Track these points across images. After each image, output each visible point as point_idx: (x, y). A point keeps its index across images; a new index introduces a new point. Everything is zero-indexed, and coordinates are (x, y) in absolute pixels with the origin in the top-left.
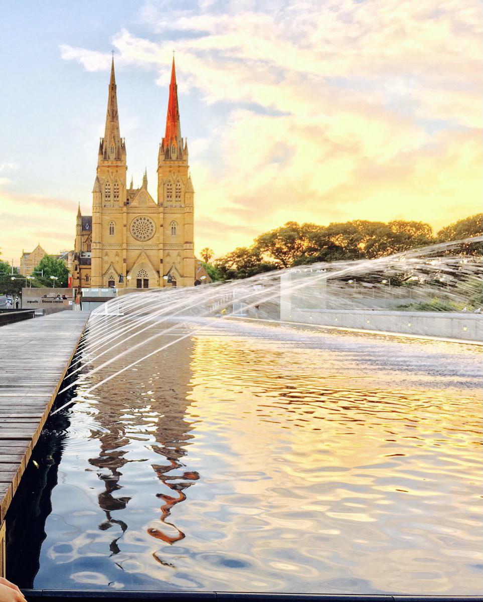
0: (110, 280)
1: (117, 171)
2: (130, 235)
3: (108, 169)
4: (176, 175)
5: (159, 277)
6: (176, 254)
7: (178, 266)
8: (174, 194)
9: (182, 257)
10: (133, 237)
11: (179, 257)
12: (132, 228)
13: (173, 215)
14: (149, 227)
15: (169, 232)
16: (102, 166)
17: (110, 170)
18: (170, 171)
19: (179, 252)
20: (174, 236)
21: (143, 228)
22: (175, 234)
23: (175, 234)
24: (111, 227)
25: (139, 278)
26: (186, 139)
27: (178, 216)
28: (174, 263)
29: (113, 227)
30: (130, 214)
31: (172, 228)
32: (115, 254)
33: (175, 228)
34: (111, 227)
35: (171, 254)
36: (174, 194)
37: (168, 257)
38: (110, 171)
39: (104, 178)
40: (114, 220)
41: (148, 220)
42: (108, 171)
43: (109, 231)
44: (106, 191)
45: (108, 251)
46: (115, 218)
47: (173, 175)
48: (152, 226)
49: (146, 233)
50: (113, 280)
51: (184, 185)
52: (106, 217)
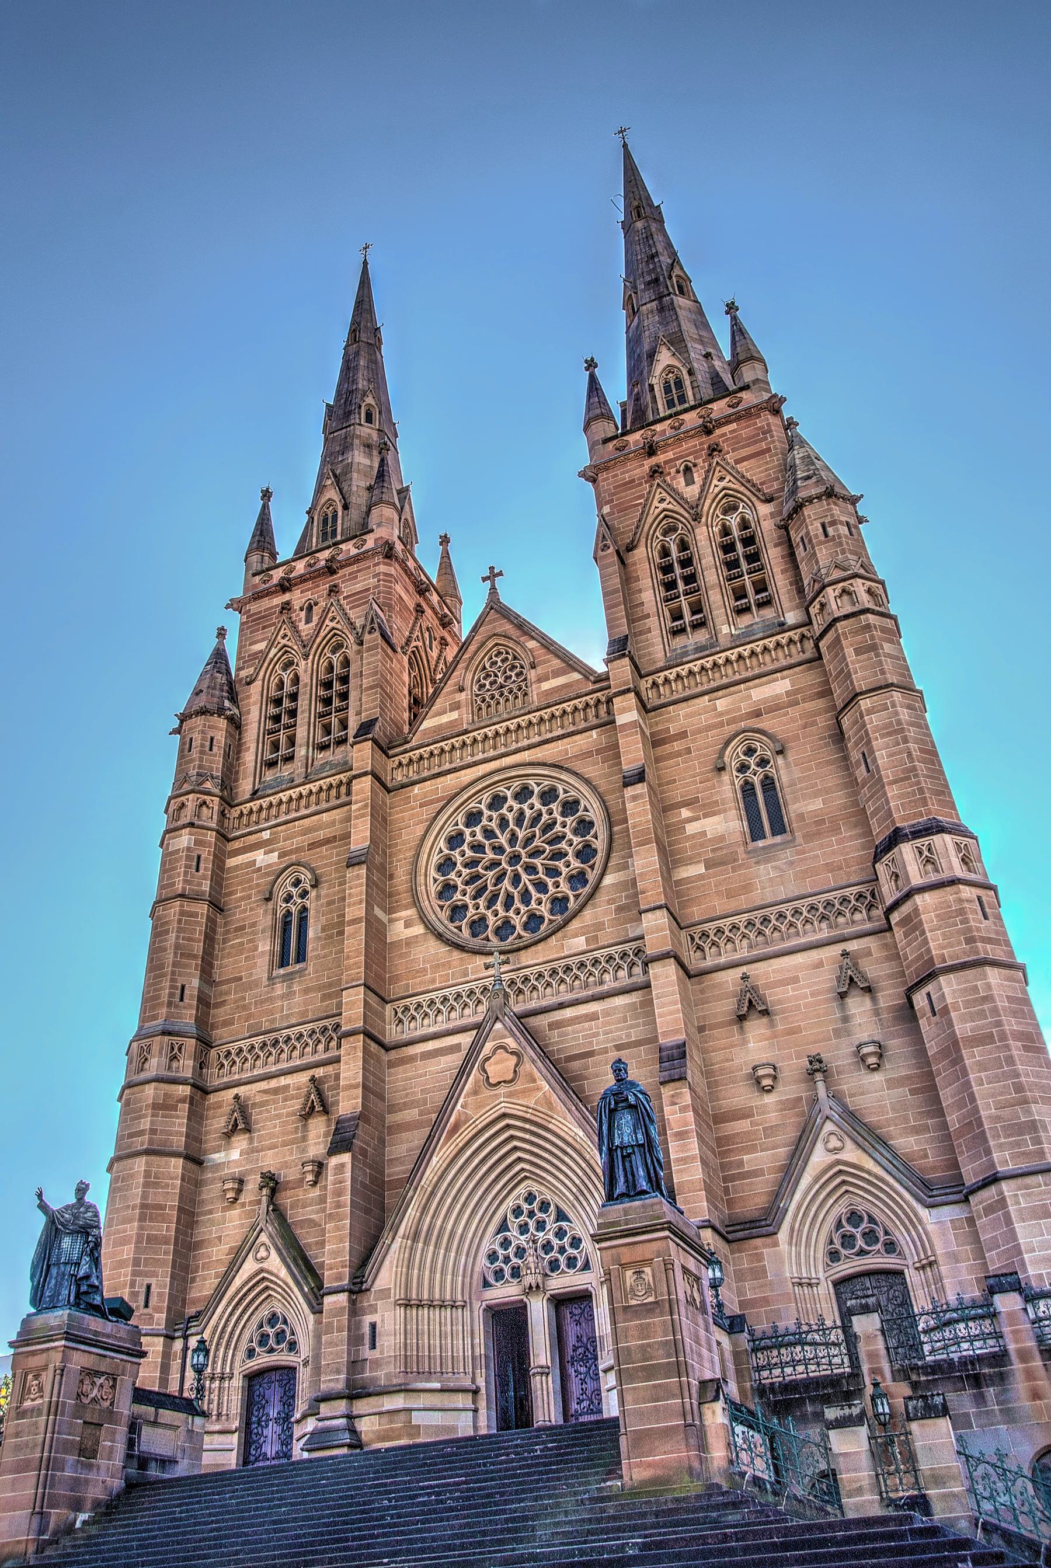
0: (263, 1360)
1: (334, 590)
2: (419, 929)
4: (698, 477)
6: (826, 979)
7: (878, 1094)
9: (889, 996)
11: (858, 1006)
12: (430, 882)
15: (726, 824)
16: (258, 596)
17: (297, 598)
18: (656, 472)
20: (778, 839)
21: (515, 859)
23: (779, 827)
24: (289, 913)
25: (506, 1292)
26: (731, 308)
27: (780, 686)
28: (817, 1067)
30: (416, 789)
31: (748, 789)
32: (297, 1105)
33: (769, 784)
34: (289, 913)
35: (772, 996)
37: (756, 1027)
39: (261, 646)
40: (305, 857)
41: (548, 796)
42: (286, 607)
43: (265, 946)
45: (241, 1090)
47: (680, 482)
48: (584, 826)
49: (541, 887)
50: (282, 1357)
51: (769, 500)
52: (260, 857)
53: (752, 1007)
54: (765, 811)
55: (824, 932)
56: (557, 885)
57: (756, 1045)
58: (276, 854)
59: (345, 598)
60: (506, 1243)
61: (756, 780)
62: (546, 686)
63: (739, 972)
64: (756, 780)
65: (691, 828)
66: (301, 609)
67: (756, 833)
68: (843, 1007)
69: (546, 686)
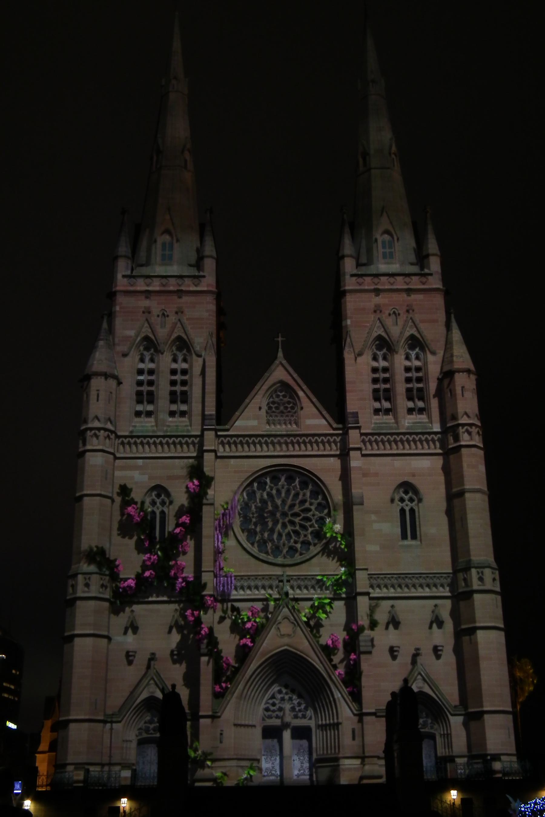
3: (146, 303)
4: (401, 322)
5: (361, 716)
8: (401, 388)
10: (245, 549)
13: (398, 462)
14: (308, 510)
19: (436, 606)
20: (414, 542)
21: (284, 514)
22: (414, 537)
27: (425, 463)
29: (163, 512)
31: (403, 511)
33: (412, 511)
36: (401, 388)
38: (156, 311)
39: (132, 333)
42: (147, 311)
44: (141, 378)
46: (170, 478)
53: (394, 622)
54: (409, 526)
55: (427, 592)
56: (305, 536)
57: (392, 637)
58: (147, 476)
59: (187, 319)
60: (274, 704)
61: (407, 509)
62: (309, 422)
63: (391, 602)
64: (407, 509)
65: (376, 526)
66: (158, 316)
67: (404, 536)
68: (431, 627)
69: (309, 422)
